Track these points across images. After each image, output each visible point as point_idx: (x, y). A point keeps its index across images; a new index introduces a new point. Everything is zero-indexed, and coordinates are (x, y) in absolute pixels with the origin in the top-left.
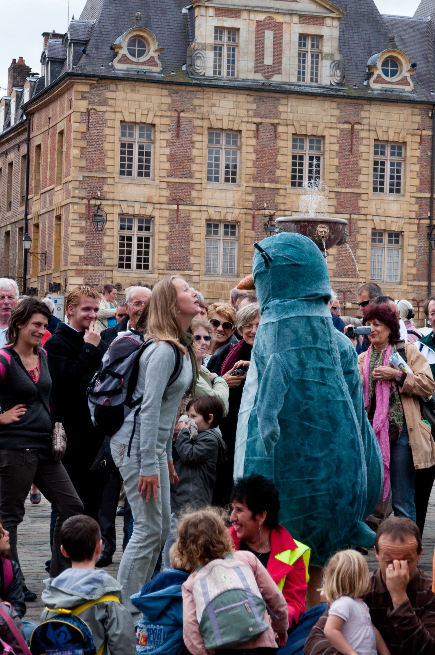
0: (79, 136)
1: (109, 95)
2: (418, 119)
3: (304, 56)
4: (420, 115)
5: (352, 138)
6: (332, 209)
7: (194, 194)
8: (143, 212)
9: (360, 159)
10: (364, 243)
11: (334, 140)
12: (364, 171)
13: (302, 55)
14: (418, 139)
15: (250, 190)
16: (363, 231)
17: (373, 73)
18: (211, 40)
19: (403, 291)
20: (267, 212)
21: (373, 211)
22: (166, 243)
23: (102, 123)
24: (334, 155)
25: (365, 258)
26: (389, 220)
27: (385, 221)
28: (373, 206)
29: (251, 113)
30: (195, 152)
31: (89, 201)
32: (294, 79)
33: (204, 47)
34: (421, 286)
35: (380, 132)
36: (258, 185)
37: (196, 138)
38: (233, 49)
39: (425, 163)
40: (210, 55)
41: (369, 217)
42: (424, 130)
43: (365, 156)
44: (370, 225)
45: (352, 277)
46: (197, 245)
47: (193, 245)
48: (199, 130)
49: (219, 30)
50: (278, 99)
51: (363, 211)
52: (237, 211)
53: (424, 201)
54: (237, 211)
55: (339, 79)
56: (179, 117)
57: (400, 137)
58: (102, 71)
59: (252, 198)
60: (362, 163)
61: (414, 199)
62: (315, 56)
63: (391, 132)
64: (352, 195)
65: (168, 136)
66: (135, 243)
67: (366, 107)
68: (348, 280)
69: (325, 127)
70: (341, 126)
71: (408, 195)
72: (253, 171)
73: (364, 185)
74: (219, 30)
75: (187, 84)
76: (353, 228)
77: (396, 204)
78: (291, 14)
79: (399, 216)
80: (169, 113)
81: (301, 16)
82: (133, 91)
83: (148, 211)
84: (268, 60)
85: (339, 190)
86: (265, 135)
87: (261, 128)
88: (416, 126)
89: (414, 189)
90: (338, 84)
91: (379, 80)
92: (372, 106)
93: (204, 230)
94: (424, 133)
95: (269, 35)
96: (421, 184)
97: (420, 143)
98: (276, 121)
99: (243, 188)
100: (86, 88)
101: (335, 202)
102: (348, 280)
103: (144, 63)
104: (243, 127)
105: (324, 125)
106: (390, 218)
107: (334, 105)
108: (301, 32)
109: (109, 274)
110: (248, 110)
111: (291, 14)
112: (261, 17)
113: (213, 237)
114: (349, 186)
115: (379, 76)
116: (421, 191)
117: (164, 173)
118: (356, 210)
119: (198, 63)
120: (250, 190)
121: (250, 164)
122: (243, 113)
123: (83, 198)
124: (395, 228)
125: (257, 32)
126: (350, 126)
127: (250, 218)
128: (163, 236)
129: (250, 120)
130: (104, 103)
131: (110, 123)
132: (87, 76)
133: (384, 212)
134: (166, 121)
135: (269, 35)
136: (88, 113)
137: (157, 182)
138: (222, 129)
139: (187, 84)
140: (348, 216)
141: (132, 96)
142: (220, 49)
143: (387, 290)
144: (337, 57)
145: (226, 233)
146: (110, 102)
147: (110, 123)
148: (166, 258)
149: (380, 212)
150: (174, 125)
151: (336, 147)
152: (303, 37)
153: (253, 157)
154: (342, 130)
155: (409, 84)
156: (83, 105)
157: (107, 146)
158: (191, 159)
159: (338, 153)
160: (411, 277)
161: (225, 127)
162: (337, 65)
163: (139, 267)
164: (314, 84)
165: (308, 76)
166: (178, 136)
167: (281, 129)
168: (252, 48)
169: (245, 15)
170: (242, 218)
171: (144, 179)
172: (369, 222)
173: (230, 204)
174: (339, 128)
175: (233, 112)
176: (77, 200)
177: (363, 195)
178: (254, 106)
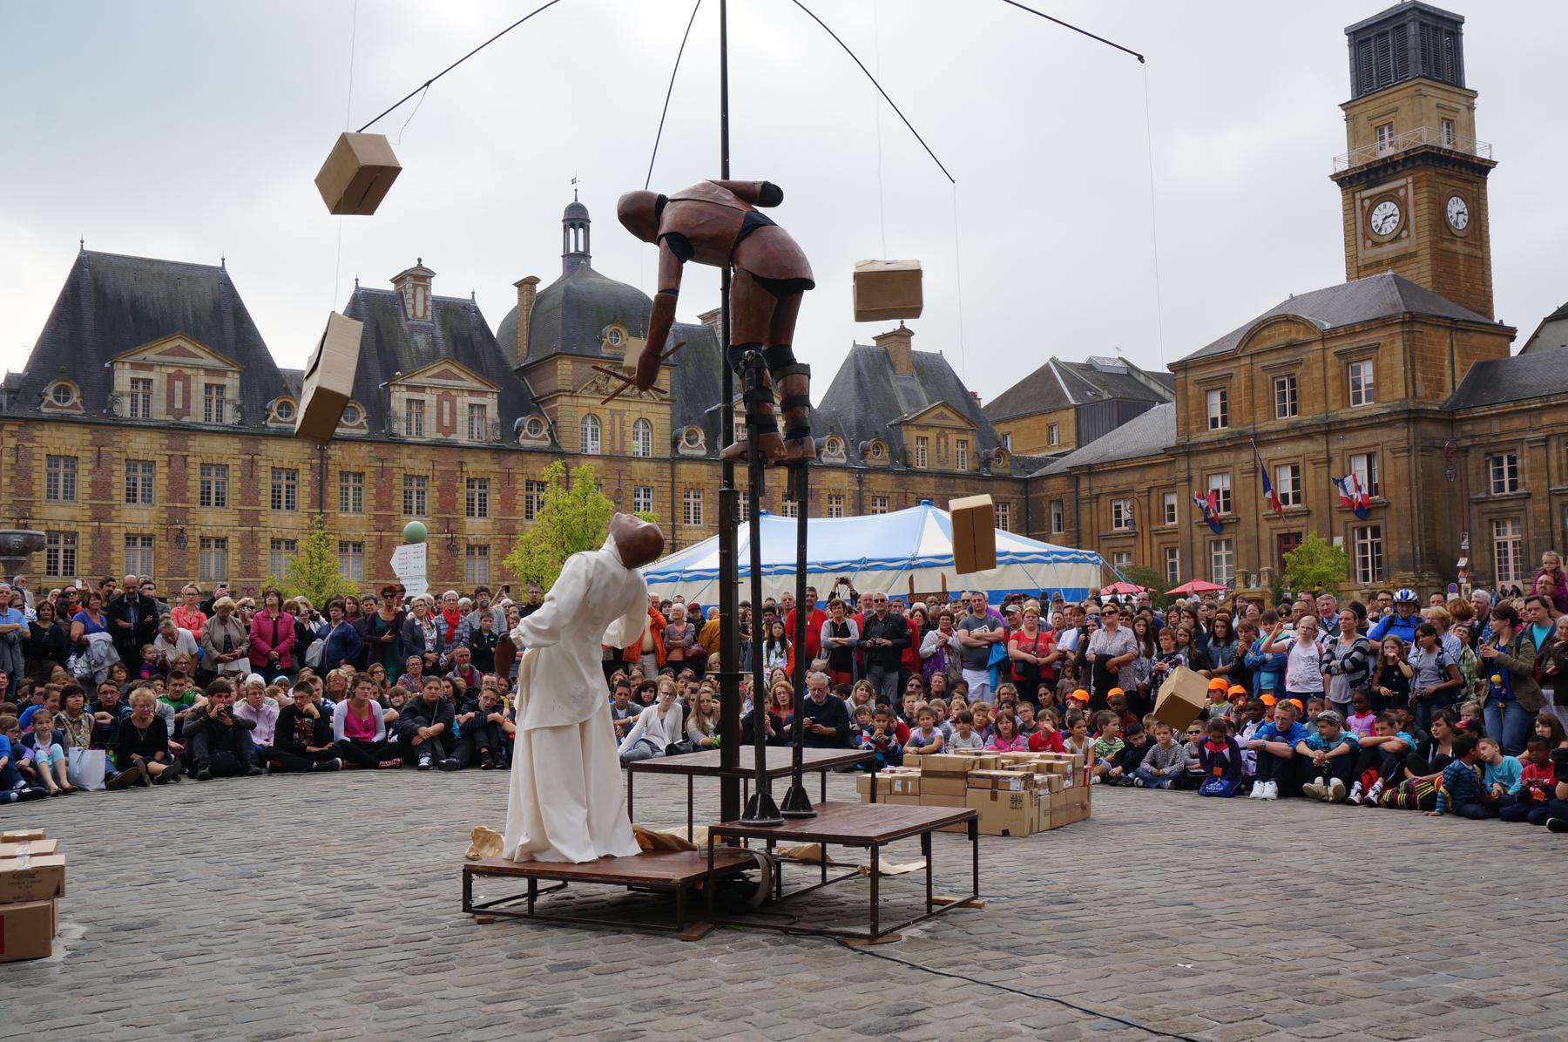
0: (9, 467)
1: (36, 433)
2: (309, 450)
3: (210, 401)
5: (252, 466)
6: (236, 523)
7: (114, 513)
8: (67, 529)
11: (237, 468)
12: (263, 492)
13: (208, 401)
15: (164, 509)
16: (263, 540)
18: (128, 389)
20: (179, 527)
21: (272, 524)
22: (89, 554)
23: (30, 456)
24: (236, 480)
26: (285, 531)
29: (164, 447)
30: (114, 479)
31: (18, 520)
32: (201, 419)
33: (122, 394)
35: (276, 461)
36: (171, 505)
37: (115, 467)
38: (147, 398)
40: (127, 401)
41: (268, 529)
43: (263, 480)
44: (269, 536)
46: (117, 555)
47: (113, 555)
48: (117, 461)
49: (134, 381)
50: (187, 436)
51: (263, 524)
52: (152, 527)
54: (152, 527)
56: (99, 451)
58: (30, 414)
59: (166, 515)
60: (261, 486)
62: (220, 403)
63: (285, 462)
65: (89, 466)
66: (61, 554)
67: (264, 442)
70: (243, 457)
71: (301, 510)
72: (166, 493)
73: (263, 504)
74: (134, 381)
75: (106, 424)
78: (198, 368)
80: (90, 448)
81: (206, 370)
82: (58, 430)
83: (73, 527)
84: (178, 405)
85: (242, 508)
86: (176, 464)
87: (172, 459)
88: (306, 456)
89: (306, 506)
90: (239, 424)
91: (275, 420)
93: (124, 542)
94: (313, 461)
95: (179, 385)
96: (312, 502)
97: (311, 470)
98: (186, 453)
99: (157, 508)
100: (15, 428)
101: (238, 518)
103: (67, 408)
104: (157, 458)
107: (236, 440)
109: (37, 581)
110: (161, 445)
111: (198, 368)
112: (172, 370)
113: (131, 548)
114: (251, 504)
115: (274, 417)
117: (86, 497)
118: (258, 524)
119: (116, 407)
120: (164, 509)
121: (164, 488)
122: (156, 447)
123: (12, 519)
124: (290, 537)
125: (168, 382)
127: (164, 532)
128: (86, 548)
129: (163, 452)
130: (32, 439)
131: (37, 457)
132: (15, 418)
134: (87, 454)
135: (179, 385)
136: (17, 448)
137: (80, 504)
138: (138, 460)
139: (106, 424)
141: (56, 433)
142: (137, 396)
144: (238, 402)
145: (143, 544)
146: (37, 439)
147: (37, 457)
148: (89, 566)
149: (278, 524)
150: (95, 457)
151: (239, 474)
152: (208, 387)
153: (167, 482)
154: (243, 460)
156: (12, 442)
157: (34, 475)
158: (111, 485)
159: (240, 478)
161: (141, 458)
162: (239, 409)
163: (65, 574)
164: (219, 423)
165: (214, 418)
166: (99, 466)
167: (190, 460)
168: (164, 395)
169: (157, 369)
170: (156, 532)
171: (69, 502)
173: (146, 520)
175: (148, 446)
176: (7, 520)
178: (167, 442)
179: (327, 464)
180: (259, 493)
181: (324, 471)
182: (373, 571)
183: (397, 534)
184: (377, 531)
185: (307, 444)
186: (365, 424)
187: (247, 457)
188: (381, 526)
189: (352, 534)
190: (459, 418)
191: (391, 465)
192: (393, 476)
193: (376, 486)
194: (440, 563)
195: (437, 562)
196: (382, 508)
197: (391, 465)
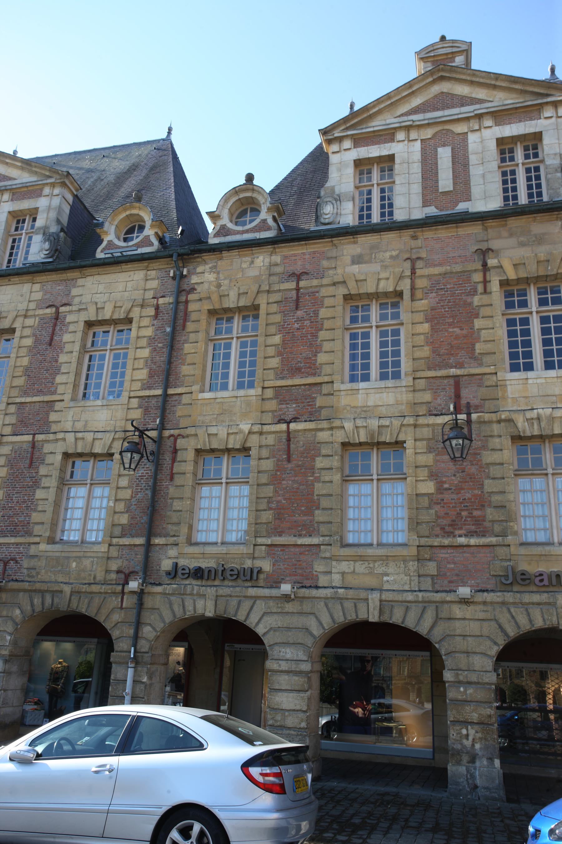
4: (158, 278)
5: (55, 325)
9: (62, 352)
10: (48, 478)
14: (151, 311)
17: (102, 241)
19: (100, 555)
25: (46, 502)
27: (83, 439)
28: (70, 418)
34: (135, 545)
39: (160, 345)
42: (163, 297)
45: (22, 536)
53: (154, 401)
55: (47, 252)
57: (122, 312)
61: (137, 400)
64: (41, 404)
68: (13, 540)
69: (17, 316)
70: (41, 312)
73: (61, 389)
76: (37, 454)
77: (105, 412)
79: (108, 429)
85: (23, 400)
92: (89, 278)
94: (161, 301)
96: (151, 375)
97: (156, 316)
102: (13, 540)
105: (15, 313)
106: (92, 434)
108: (11, 209)
114: (40, 392)
116: (150, 388)
126: (54, 309)
133: (85, 426)
140: (29, 438)
143: (74, 554)
149: (79, 426)
155: (152, 244)
160: (117, 531)
172: (60, 443)
174: (38, 315)
177: (57, 403)
179: (187, 302)
180: (57, 371)
181: (181, 314)
182: (268, 516)
183: (325, 424)
184: (279, 422)
185: (153, 274)
186: (270, 222)
187: (48, 311)
188: (291, 410)
189: (222, 432)
190: (475, 171)
191: (315, 282)
192: (318, 303)
193: (282, 328)
194: (440, 489)
195: (429, 487)
196: (296, 371)
197: (315, 282)
